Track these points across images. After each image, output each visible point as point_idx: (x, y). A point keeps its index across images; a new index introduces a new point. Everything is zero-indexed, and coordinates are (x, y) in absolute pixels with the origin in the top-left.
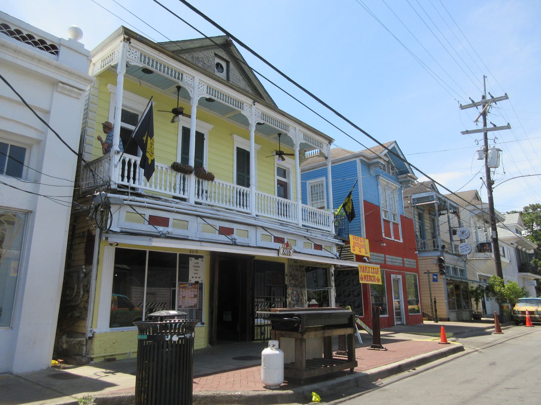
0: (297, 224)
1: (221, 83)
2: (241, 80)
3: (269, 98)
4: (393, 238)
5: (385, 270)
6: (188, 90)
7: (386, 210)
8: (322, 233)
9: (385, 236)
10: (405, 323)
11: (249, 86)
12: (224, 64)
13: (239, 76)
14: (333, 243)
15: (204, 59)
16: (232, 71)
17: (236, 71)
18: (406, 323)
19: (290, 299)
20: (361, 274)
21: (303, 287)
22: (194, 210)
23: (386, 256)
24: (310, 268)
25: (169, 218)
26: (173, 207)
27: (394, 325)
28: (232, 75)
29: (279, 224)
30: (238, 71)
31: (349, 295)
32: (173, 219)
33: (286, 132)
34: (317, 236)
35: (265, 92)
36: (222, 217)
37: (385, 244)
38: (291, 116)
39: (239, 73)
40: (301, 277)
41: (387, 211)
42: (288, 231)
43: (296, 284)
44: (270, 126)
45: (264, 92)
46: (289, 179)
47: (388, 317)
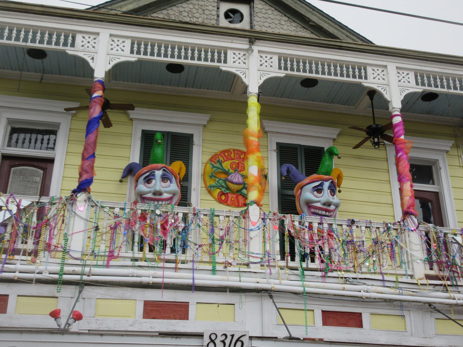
0: (412, 276)
1: (159, 28)
2: (283, 23)
3: (354, 35)
6: (86, 57)
11: (303, 27)
12: (244, 9)
13: (278, 17)
15: (194, 11)
16: (258, 15)
17: (270, 12)
22: (70, 272)
25: (7, 296)
26: (15, 272)
28: (259, 19)
30: (276, 9)
32: (18, 296)
33: (360, 80)
35: (340, 27)
36: (145, 280)
38: (404, 50)
39: (276, 12)
42: (362, 294)
44: (343, 83)
45: (338, 28)
46: (440, 183)
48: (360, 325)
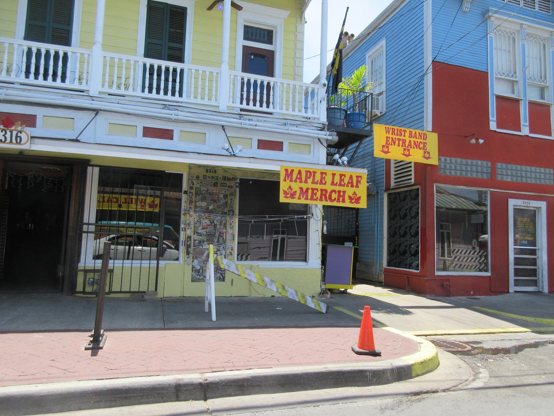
4: (525, 131)
5: (491, 192)
7: (513, 79)
8: (284, 121)
9: (498, 127)
10: (546, 290)
14: (314, 138)
18: (549, 292)
19: (189, 232)
20: (284, 186)
21: (231, 212)
23: (499, 165)
24: (251, 182)
27: (508, 292)
29: (162, 106)
31: (405, 233)
34: (258, 124)
37: (481, 141)
40: (226, 196)
41: (517, 82)
42: (173, 117)
43: (211, 207)
47: (490, 277)
48: (171, 138)
